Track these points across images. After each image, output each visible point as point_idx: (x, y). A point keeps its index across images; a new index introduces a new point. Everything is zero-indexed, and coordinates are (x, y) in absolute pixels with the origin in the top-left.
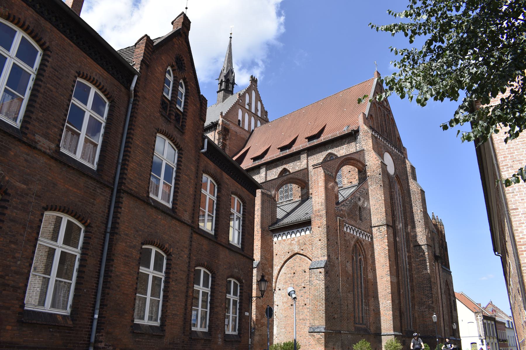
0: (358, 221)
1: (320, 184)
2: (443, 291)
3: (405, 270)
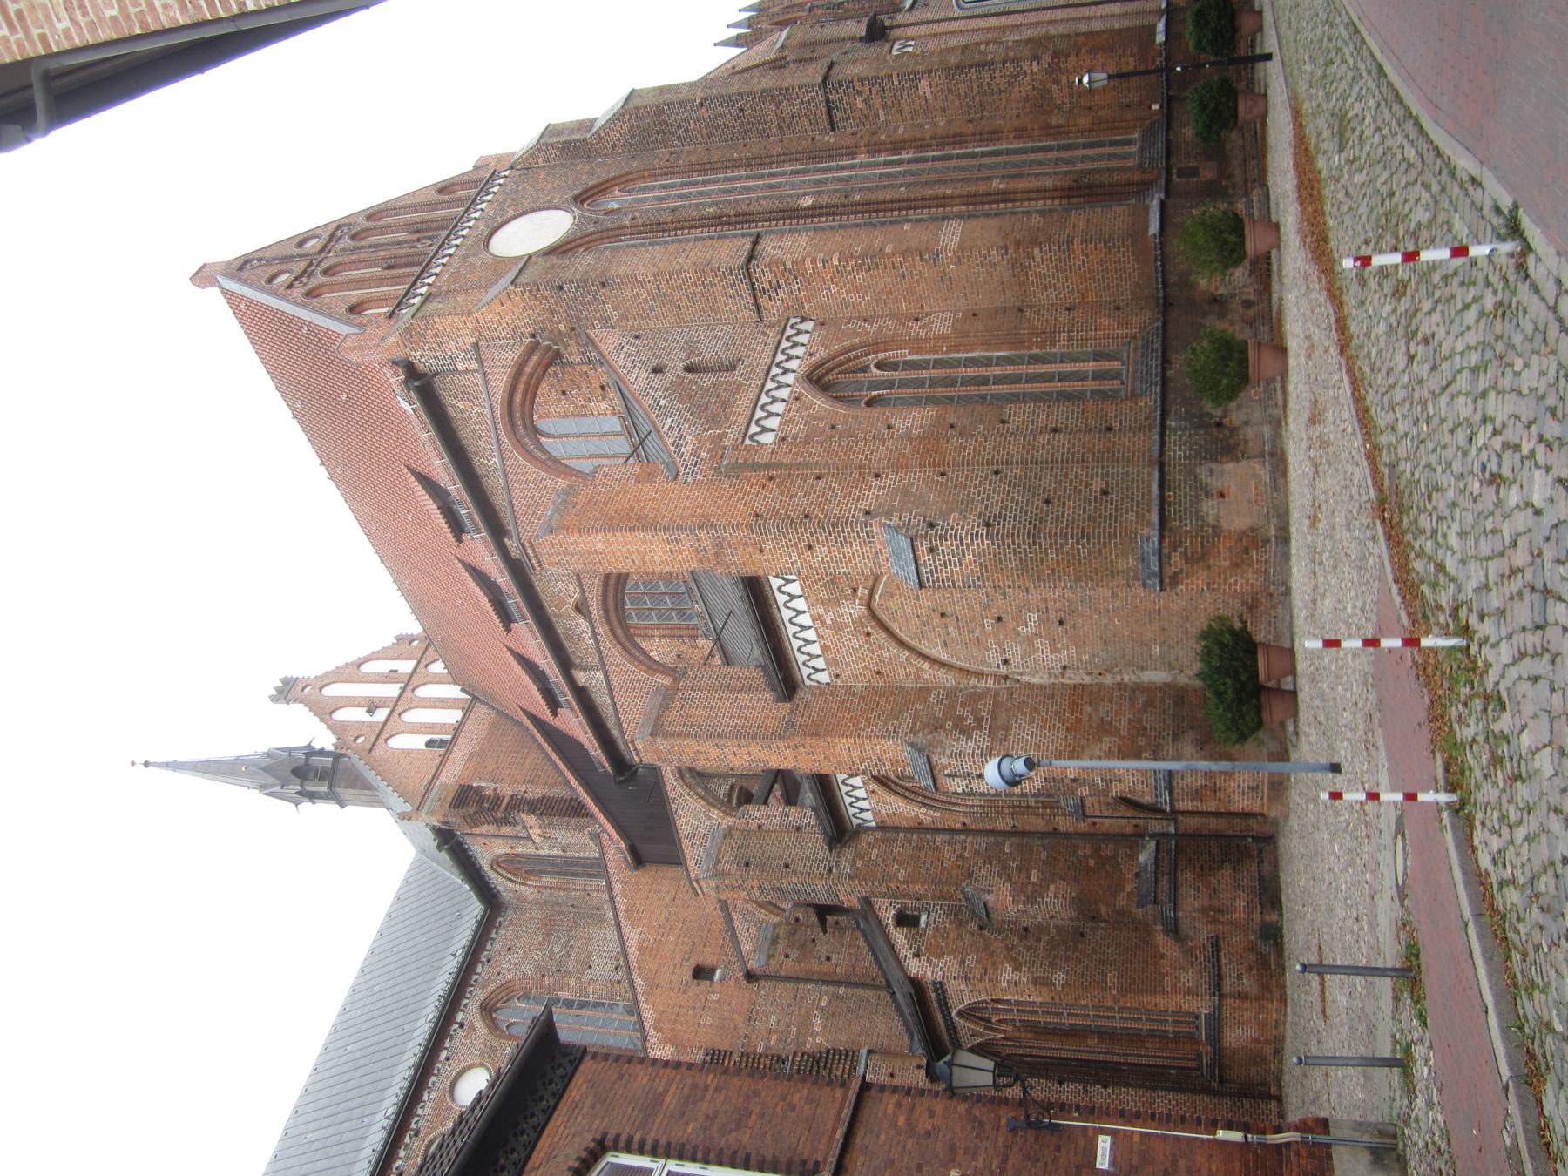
0: (737, 375)
1: (600, 547)
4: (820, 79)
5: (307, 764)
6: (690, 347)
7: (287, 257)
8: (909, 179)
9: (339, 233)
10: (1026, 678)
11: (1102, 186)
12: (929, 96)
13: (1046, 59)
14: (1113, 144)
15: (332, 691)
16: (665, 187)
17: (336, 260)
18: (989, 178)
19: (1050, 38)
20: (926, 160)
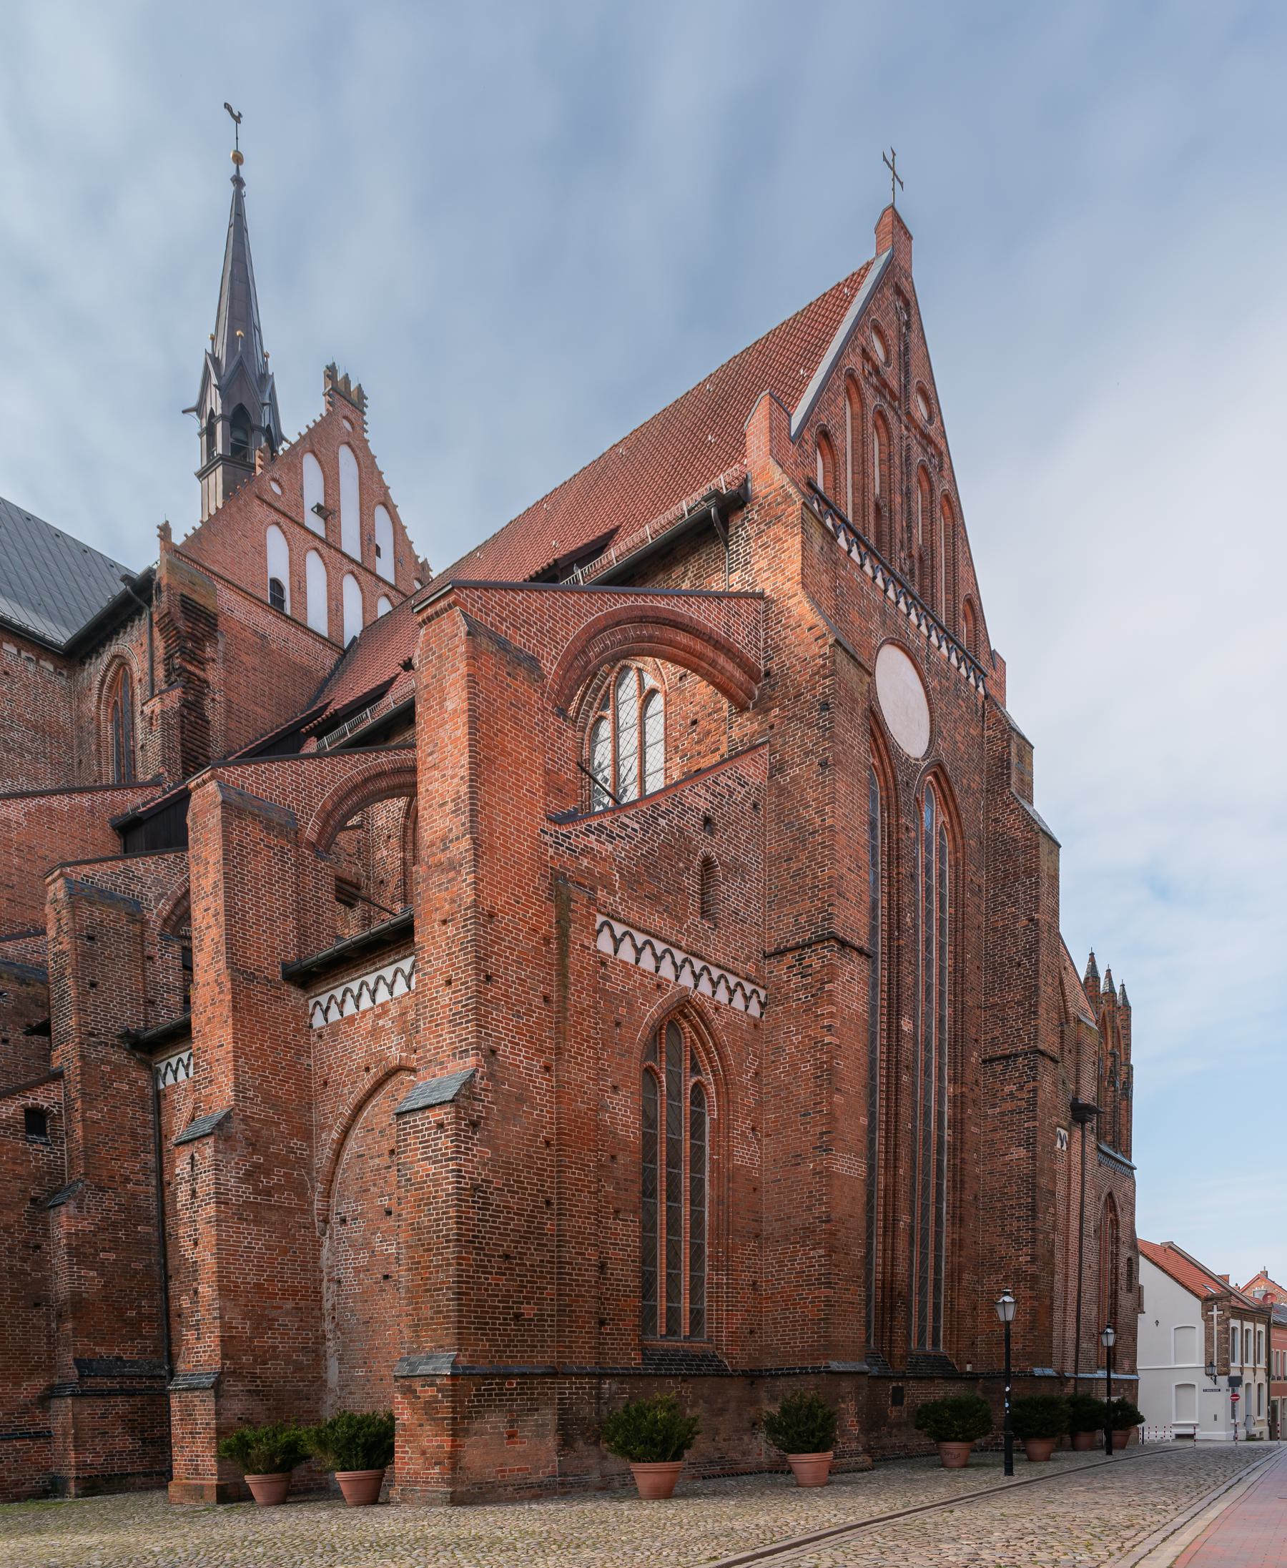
2: (1090, 1227)
4: (1041, 1047)
5: (254, 428)
6: (736, 869)
7: (907, 365)
8: (920, 1135)
9: (931, 450)
10: (327, 1243)
12: (1007, 1158)
13: (1031, 1269)
15: (346, 459)
16: (941, 876)
17: (895, 433)
19: (1052, 1274)
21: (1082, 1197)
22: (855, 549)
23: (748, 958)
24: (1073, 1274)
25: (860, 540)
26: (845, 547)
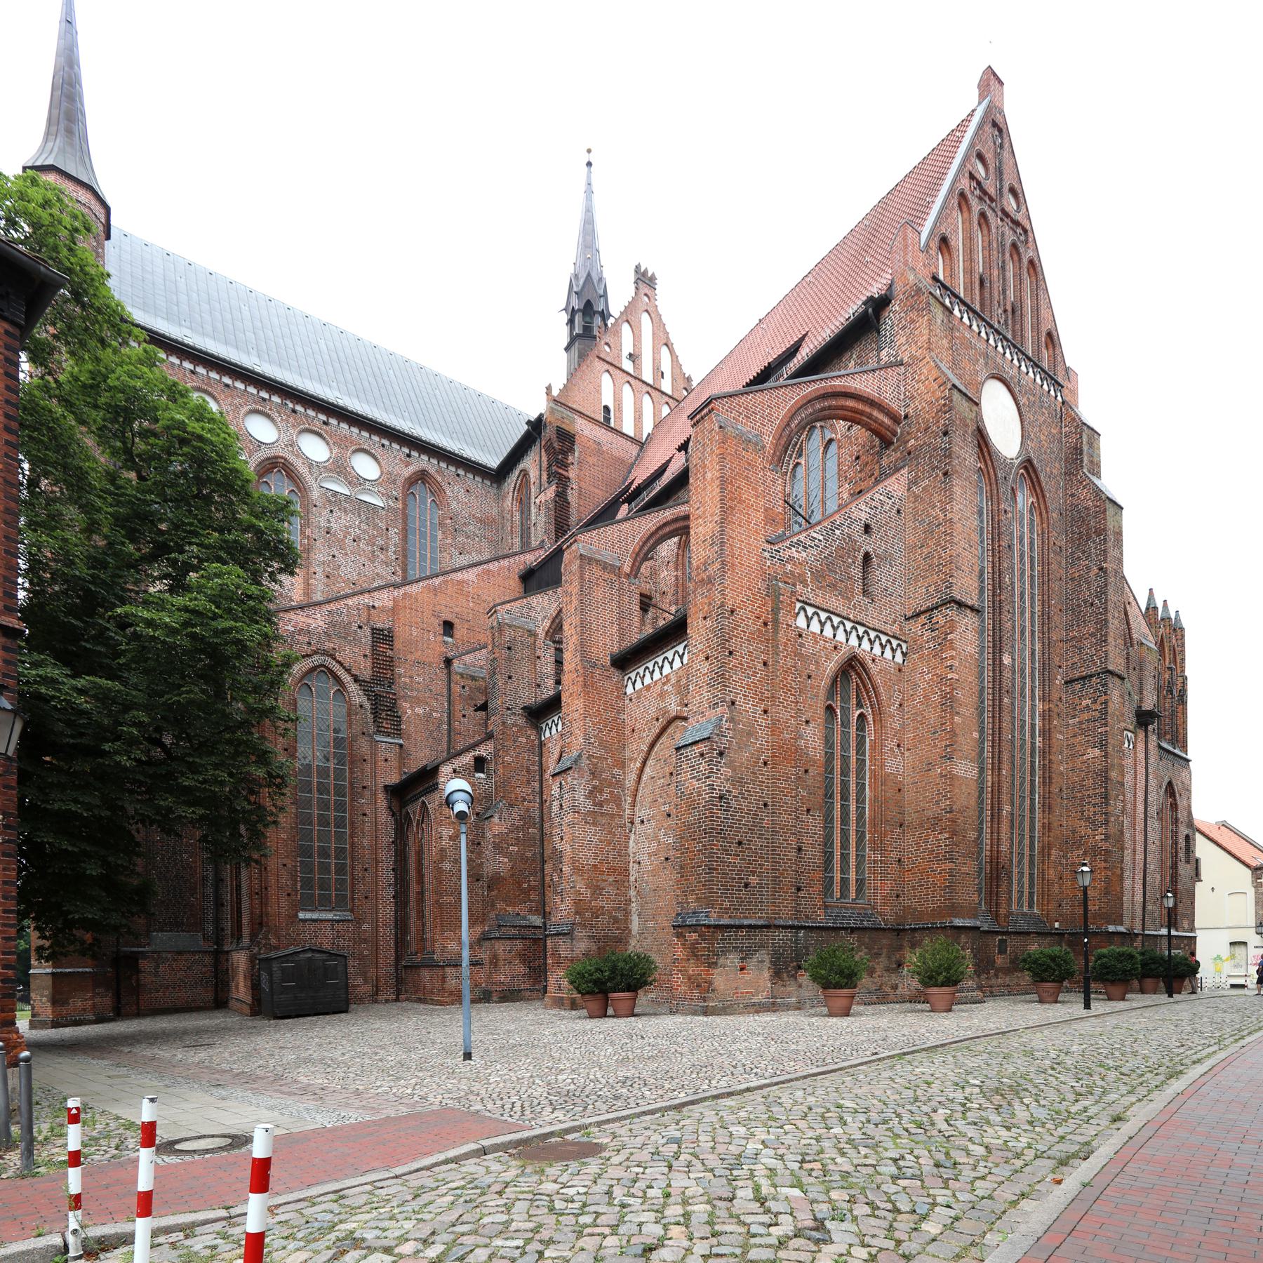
2: (1153, 810)
3: (1028, 752)
4: (1110, 668)
7: (1001, 173)
9: (1019, 230)
11: (998, 886)
14: (1031, 894)
16: (1032, 543)
18: (1012, 804)
20: (1032, 756)
21: (1146, 786)
22: (965, 316)
23: (895, 621)
24: (1140, 849)
25: (970, 309)
26: (959, 315)
